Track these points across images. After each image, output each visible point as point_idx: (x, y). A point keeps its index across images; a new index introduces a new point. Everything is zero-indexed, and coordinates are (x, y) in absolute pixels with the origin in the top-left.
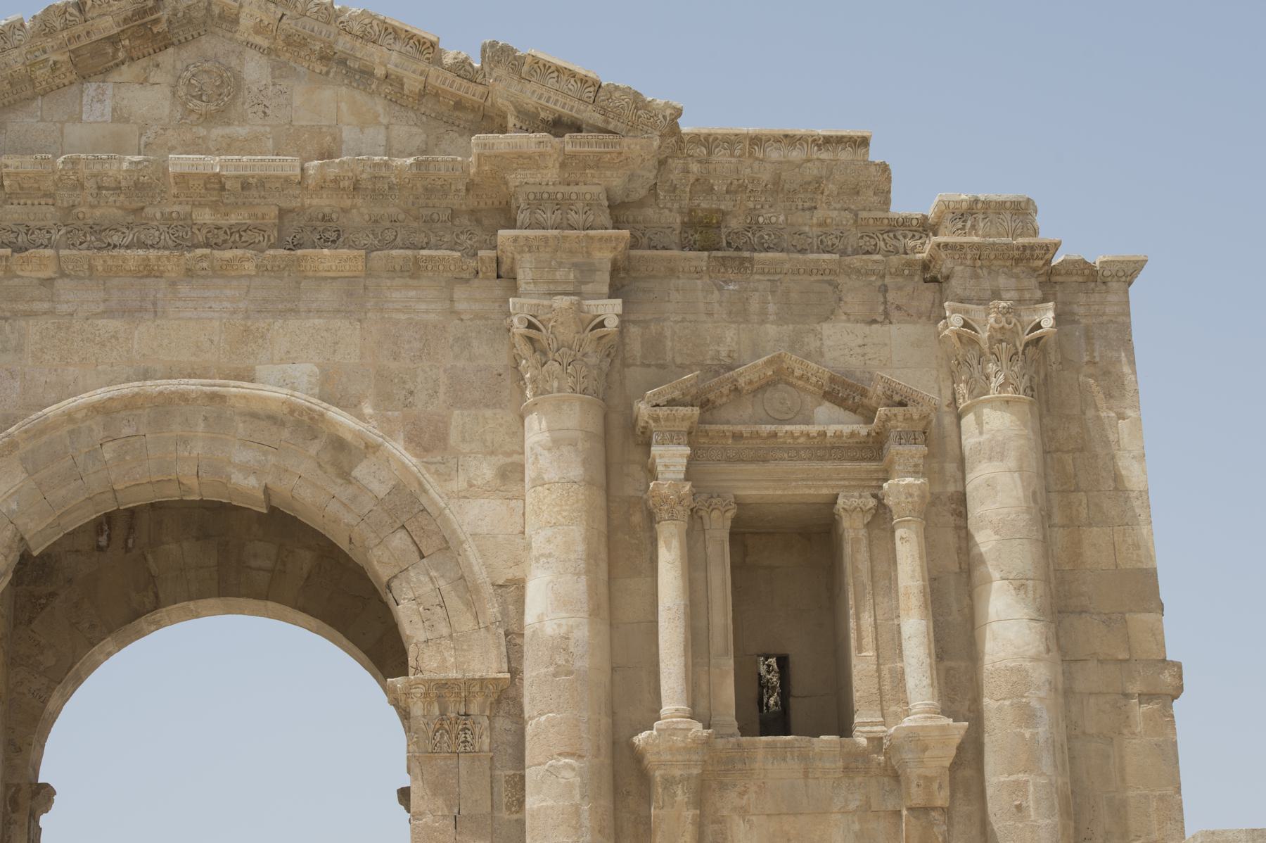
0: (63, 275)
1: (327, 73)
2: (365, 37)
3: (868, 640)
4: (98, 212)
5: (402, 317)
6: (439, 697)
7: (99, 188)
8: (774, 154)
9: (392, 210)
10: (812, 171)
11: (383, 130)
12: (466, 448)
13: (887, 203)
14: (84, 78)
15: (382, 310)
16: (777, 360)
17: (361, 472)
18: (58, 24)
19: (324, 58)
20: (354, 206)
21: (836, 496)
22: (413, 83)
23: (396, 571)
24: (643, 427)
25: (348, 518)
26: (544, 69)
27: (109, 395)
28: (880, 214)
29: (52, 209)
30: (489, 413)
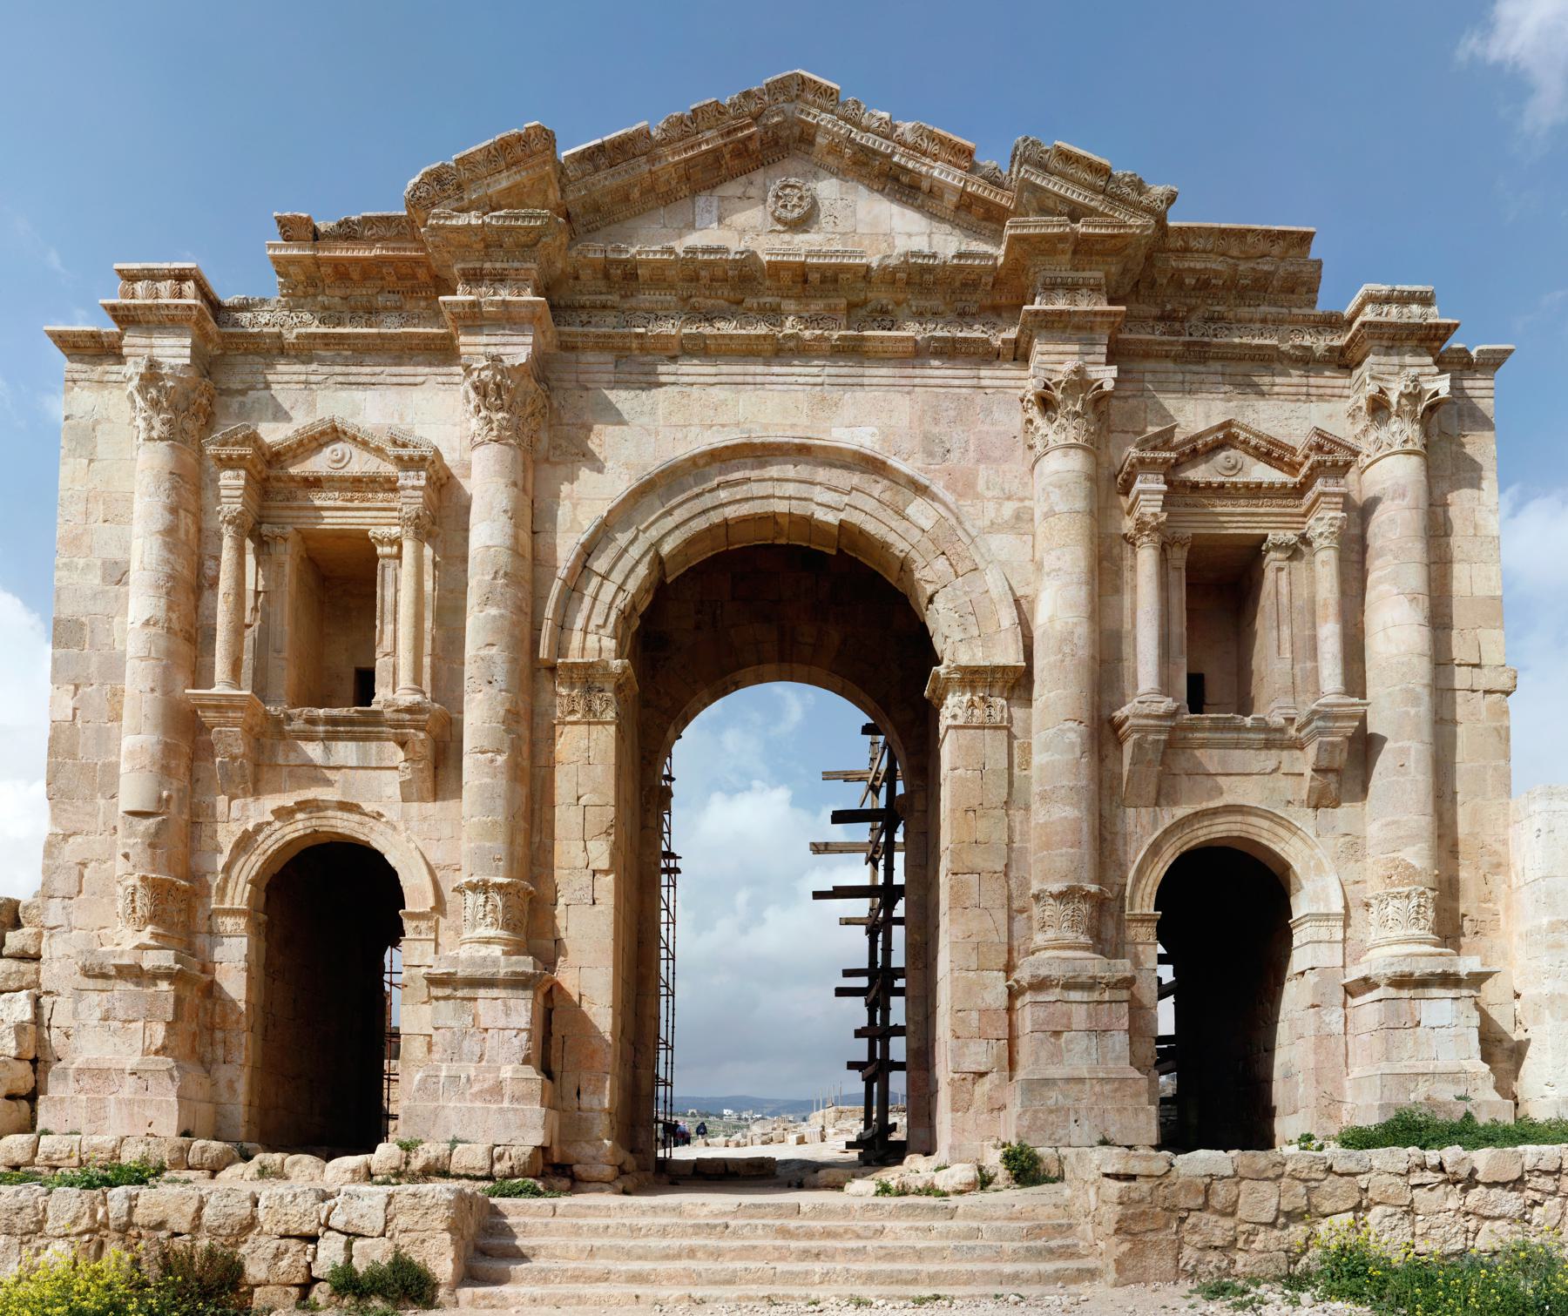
3: (1286, 646)
4: (710, 302)
5: (942, 390)
7: (712, 280)
11: (926, 238)
12: (989, 494)
13: (1313, 303)
14: (695, 193)
16: (1228, 424)
21: (1266, 536)
23: (938, 587)
25: (900, 546)
28: (1307, 311)
29: (675, 299)
30: (1005, 467)
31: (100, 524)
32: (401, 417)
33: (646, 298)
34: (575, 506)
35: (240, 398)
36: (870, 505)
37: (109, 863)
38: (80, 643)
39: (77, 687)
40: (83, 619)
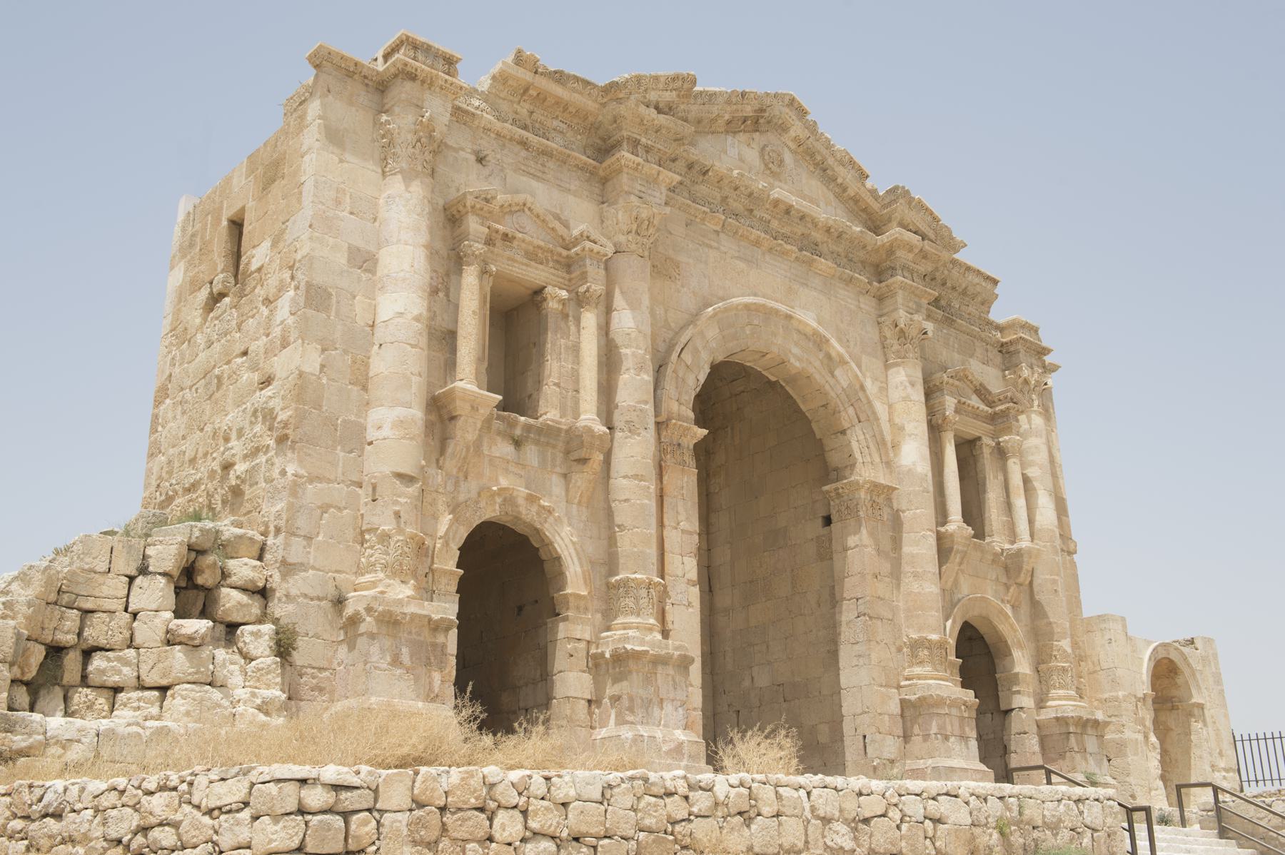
0: (723, 232)
1: (814, 173)
2: (841, 163)
6: (872, 491)
8: (971, 277)
9: (840, 250)
10: (978, 289)
13: (989, 312)
14: (727, 132)
15: (836, 297)
17: (837, 373)
18: (734, 100)
19: (816, 165)
20: (827, 242)
21: (979, 438)
22: (851, 192)
23: (849, 426)
24: (935, 385)
25: (833, 394)
26: (921, 207)
27: (754, 301)
30: (874, 360)
31: (346, 214)
32: (561, 210)
33: (703, 189)
34: (666, 311)
35: (454, 154)
36: (817, 364)
37: (345, 512)
38: (327, 309)
39: (323, 350)
40: (331, 290)
